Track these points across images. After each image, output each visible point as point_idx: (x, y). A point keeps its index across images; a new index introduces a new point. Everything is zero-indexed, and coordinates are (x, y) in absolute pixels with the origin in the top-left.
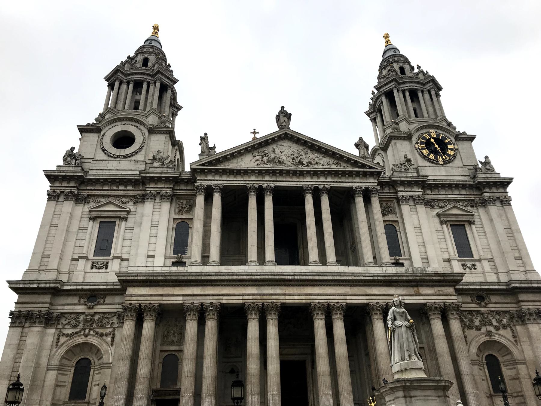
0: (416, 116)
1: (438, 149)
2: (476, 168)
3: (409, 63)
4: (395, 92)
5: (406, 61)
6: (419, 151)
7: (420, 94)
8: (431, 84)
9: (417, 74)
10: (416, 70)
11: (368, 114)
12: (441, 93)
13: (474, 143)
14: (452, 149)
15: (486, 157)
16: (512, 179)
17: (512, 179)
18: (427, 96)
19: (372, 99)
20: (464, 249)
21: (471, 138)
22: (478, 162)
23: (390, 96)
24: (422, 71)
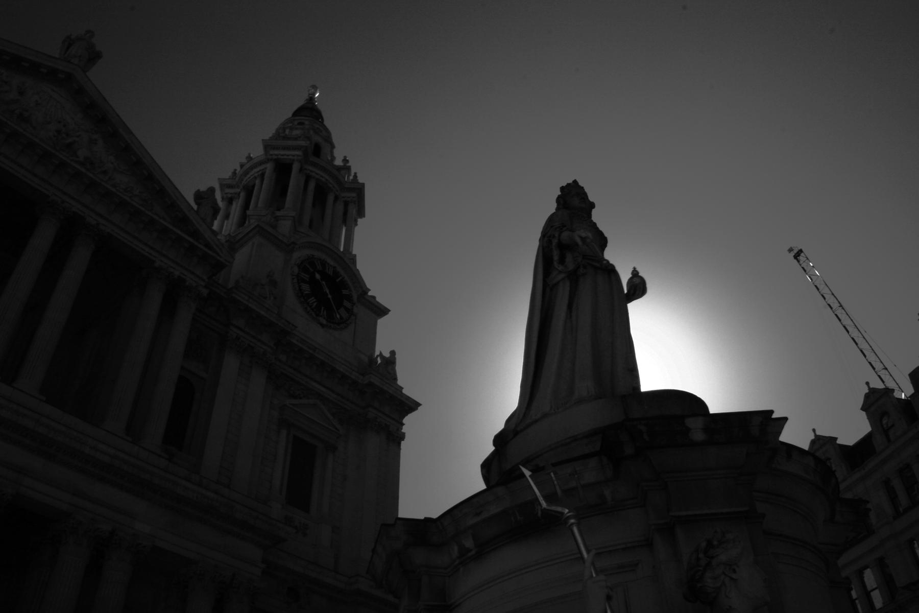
0: (311, 226)
1: (330, 296)
2: (372, 361)
3: (333, 146)
4: (296, 167)
5: (328, 139)
6: (295, 280)
7: (331, 198)
8: (354, 195)
9: (339, 169)
10: (338, 162)
11: (223, 186)
12: (359, 220)
13: (381, 322)
14: (347, 310)
15: (393, 353)
16: (419, 405)
17: (419, 405)
18: (340, 207)
19: (242, 166)
20: (299, 491)
21: (382, 311)
22: (377, 353)
23: (283, 169)
24: (348, 169)
